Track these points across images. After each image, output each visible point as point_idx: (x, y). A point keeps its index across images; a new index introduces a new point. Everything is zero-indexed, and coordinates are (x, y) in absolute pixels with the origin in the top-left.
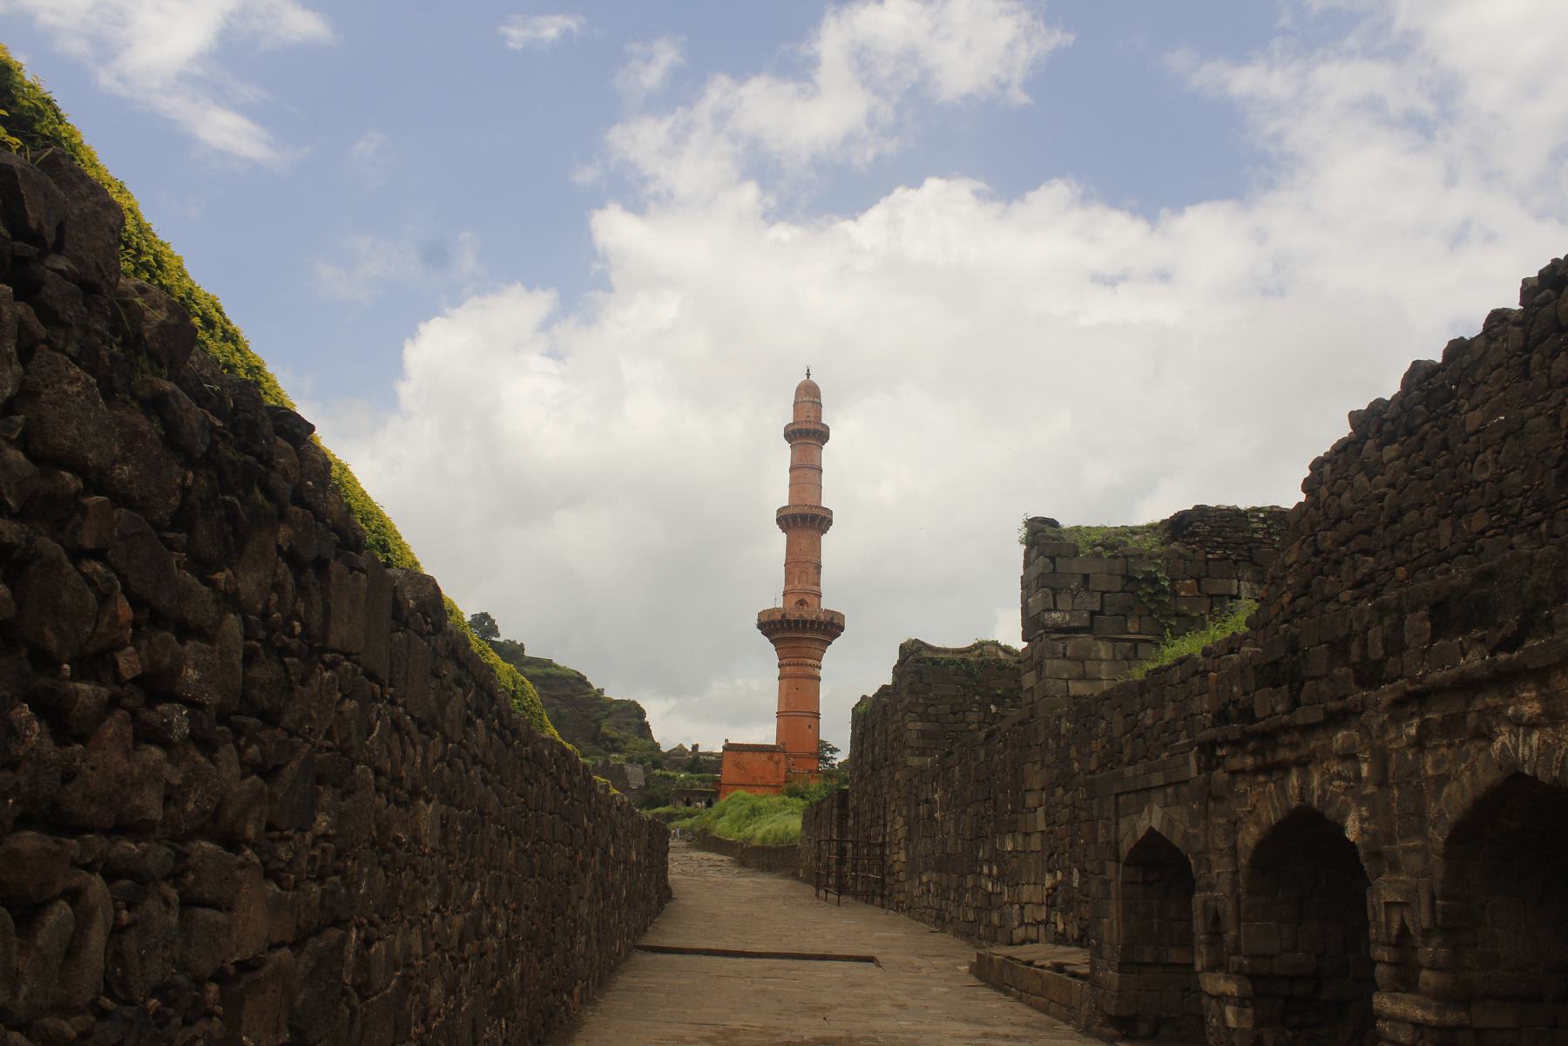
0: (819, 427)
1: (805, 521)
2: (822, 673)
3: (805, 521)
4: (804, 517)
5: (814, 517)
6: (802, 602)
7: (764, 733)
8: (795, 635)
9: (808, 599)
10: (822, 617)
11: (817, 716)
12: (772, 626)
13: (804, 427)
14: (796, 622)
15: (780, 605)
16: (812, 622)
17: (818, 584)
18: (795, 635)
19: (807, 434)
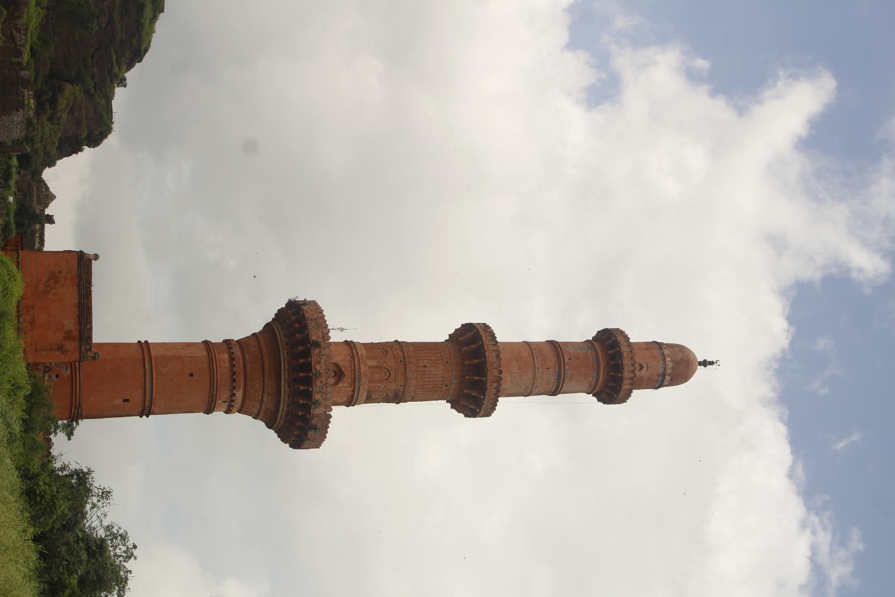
0: (626, 386)
1: (469, 371)
2: (218, 416)
3: (469, 371)
5: (480, 386)
6: (339, 374)
7: (111, 325)
8: (284, 365)
9: (344, 385)
11: (145, 412)
12: (297, 325)
13: (626, 362)
14: (308, 367)
15: (335, 337)
16: (308, 395)
17: (369, 400)
18: (284, 365)
19: (612, 367)
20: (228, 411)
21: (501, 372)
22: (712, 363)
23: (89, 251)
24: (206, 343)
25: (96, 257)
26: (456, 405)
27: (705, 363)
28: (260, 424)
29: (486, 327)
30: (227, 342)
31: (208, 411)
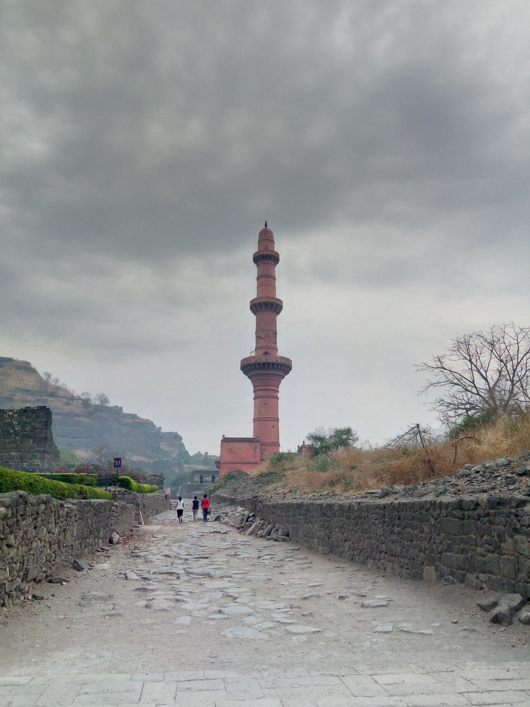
2: (279, 395)
4: (266, 304)
6: (266, 353)
10: (279, 362)
12: (249, 368)
13: (265, 253)
14: (264, 364)
15: (253, 354)
17: (276, 343)
20: (278, 392)
21: (267, 297)
22: (266, 223)
23: (221, 438)
24: (254, 399)
25: (224, 436)
26: (278, 313)
27: (266, 225)
28: (283, 381)
29: (251, 302)
30: (254, 391)
31: (278, 398)
